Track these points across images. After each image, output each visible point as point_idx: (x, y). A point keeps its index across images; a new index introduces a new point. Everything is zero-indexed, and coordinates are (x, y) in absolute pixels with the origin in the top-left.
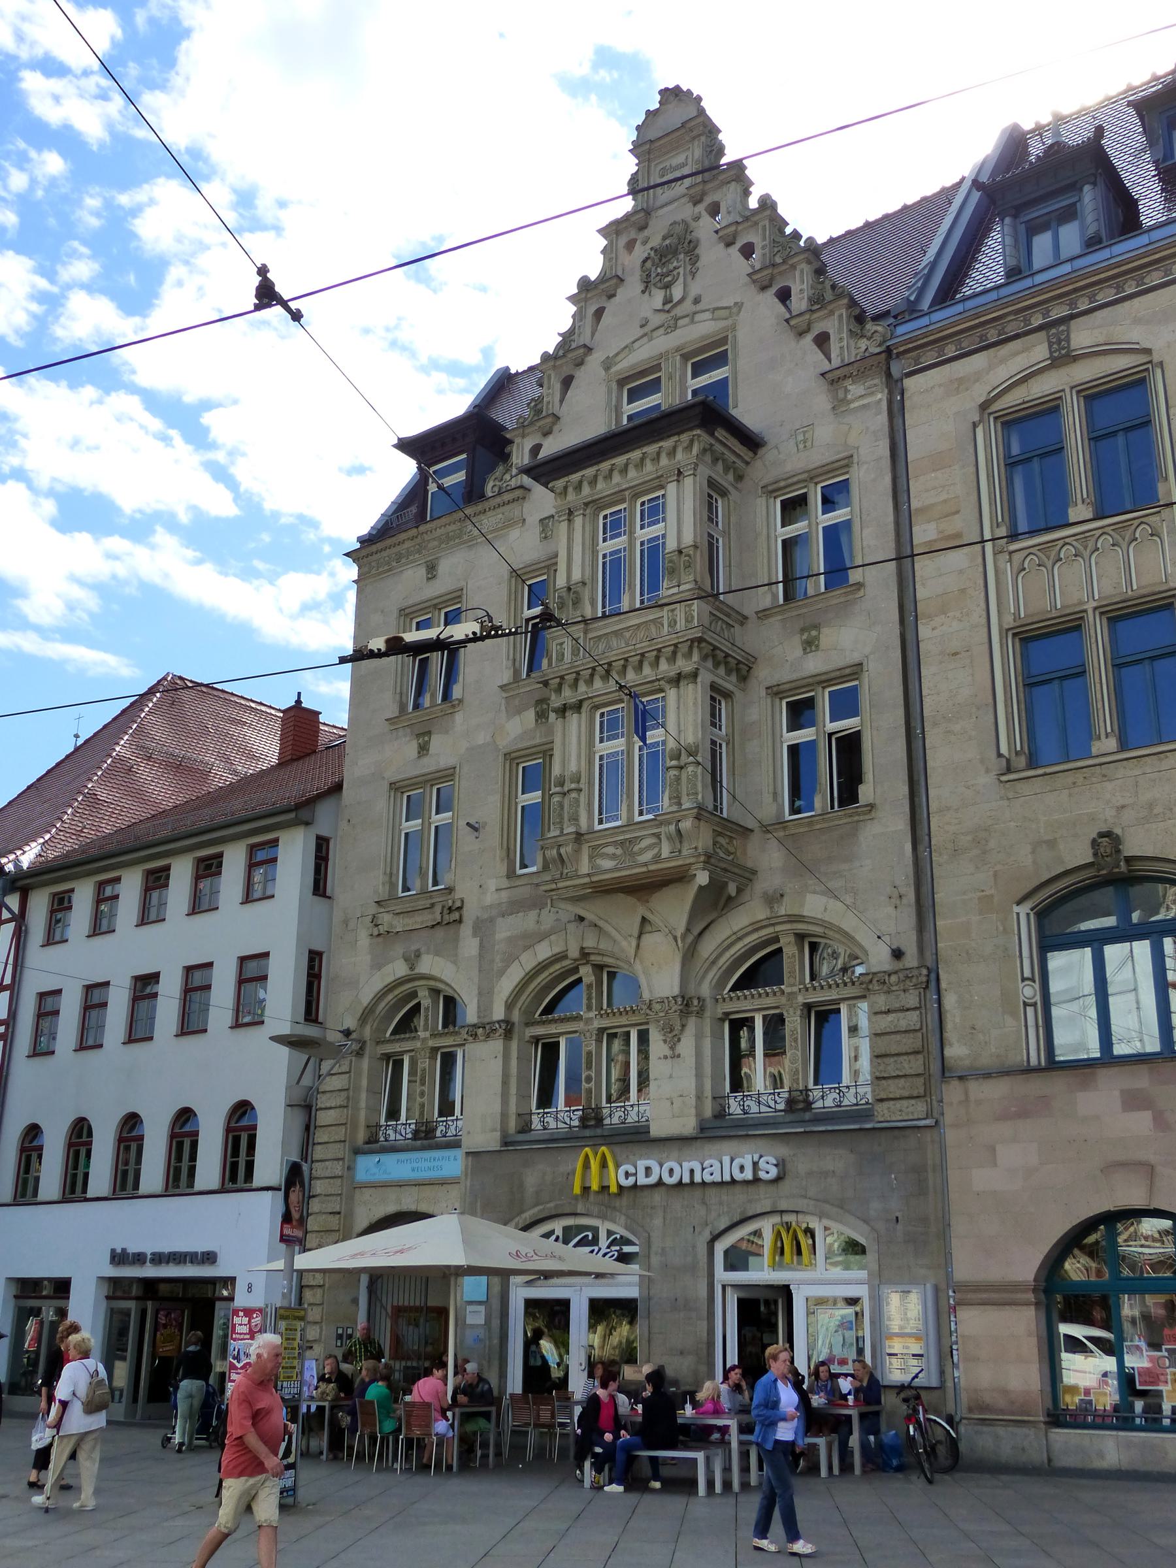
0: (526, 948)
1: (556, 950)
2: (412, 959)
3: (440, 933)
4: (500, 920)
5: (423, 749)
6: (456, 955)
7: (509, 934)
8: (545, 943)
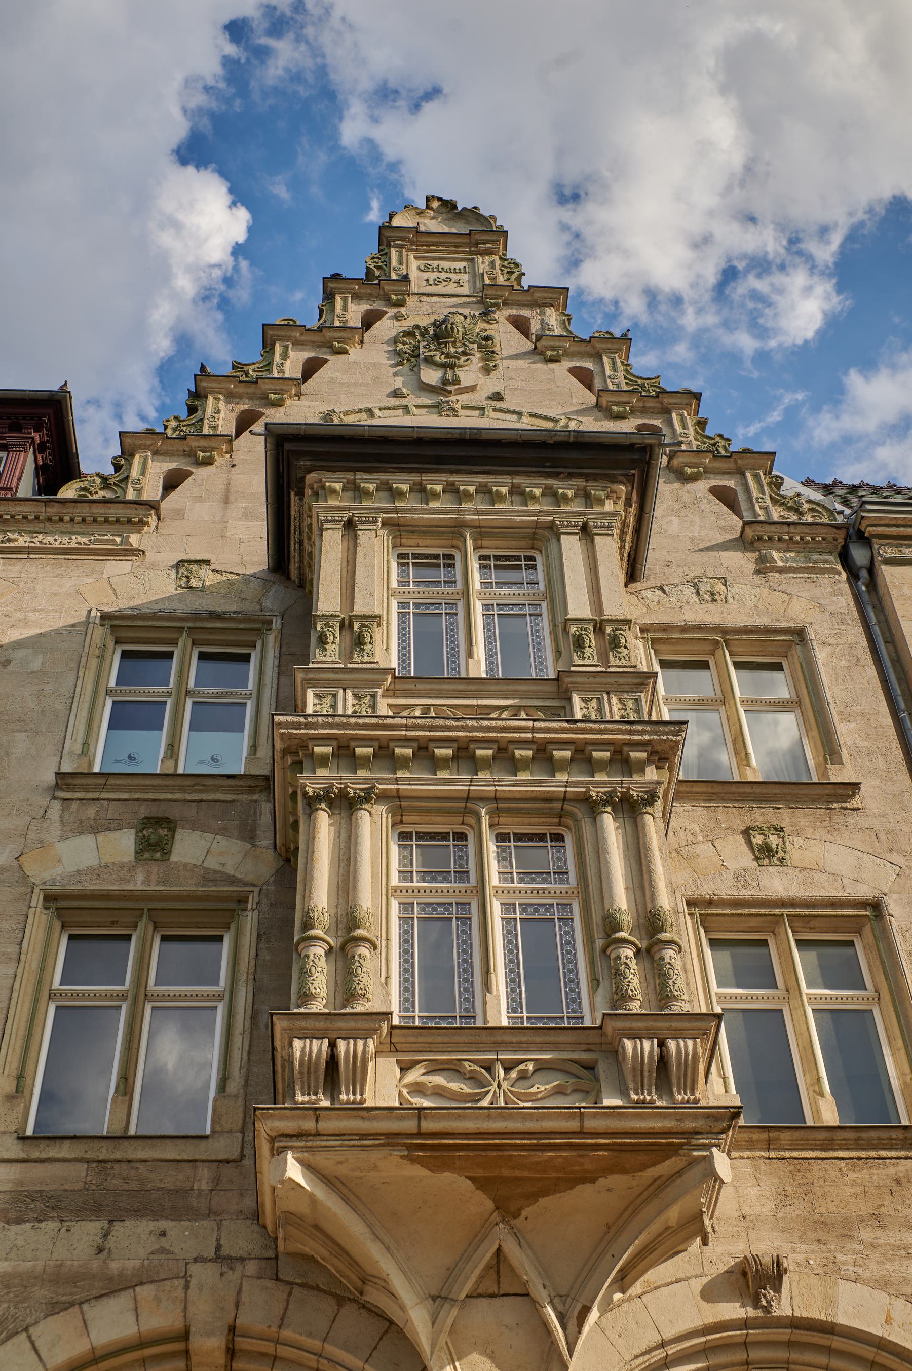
0: (55, 1308)
8: (123, 1300)
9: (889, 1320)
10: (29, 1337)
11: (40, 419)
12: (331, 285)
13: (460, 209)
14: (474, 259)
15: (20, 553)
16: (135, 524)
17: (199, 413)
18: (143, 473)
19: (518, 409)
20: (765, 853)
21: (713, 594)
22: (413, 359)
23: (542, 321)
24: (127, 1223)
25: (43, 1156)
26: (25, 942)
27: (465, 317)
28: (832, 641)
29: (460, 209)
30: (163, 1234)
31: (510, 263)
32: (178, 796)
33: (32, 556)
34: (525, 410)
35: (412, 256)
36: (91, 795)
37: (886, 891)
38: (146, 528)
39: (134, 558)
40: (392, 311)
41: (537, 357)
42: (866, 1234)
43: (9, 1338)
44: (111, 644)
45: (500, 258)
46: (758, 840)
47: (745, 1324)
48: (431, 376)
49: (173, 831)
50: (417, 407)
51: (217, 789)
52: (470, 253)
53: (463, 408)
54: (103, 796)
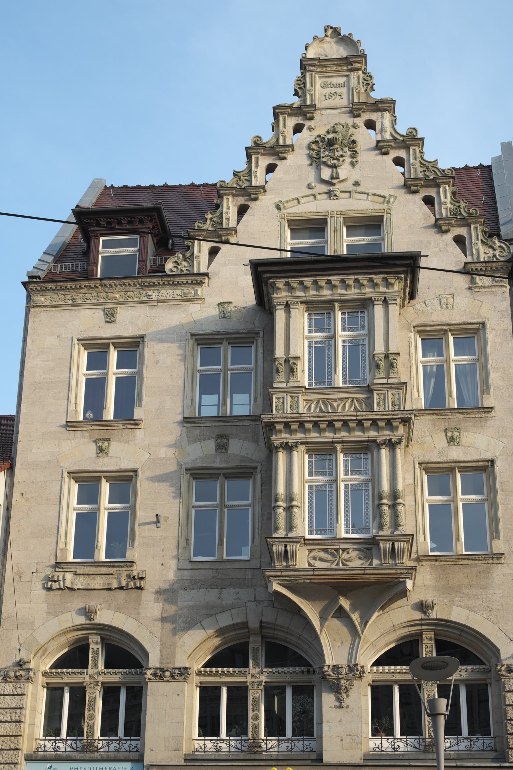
0: (208, 616)
1: (237, 621)
2: (88, 613)
3: (121, 595)
4: (181, 592)
5: (101, 451)
6: (138, 613)
7: (191, 603)
8: (228, 613)
9: (468, 619)
10: (201, 625)
11: (151, 217)
12: (277, 111)
13: (342, 35)
14: (349, 75)
15: (154, 303)
16: (199, 283)
17: (220, 208)
18: (200, 252)
19: (367, 191)
20: (451, 440)
21: (447, 304)
22: (317, 161)
23: (382, 123)
24: (226, 589)
25: (198, 568)
26: (181, 489)
27: (343, 127)
28: (496, 328)
29: (342, 35)
30: (238, 593)
31: (367, 76)
32: (229, 424)
33: (159, 304)
34: (370, 191)
35: (317, 78)
36: (197, 425)
37: (497, 455)
38: (204, 284)
39: (201, 302)
40: (307, 124)
41: (377, 152)
42: (465, 591)
43: (195, 625)
44: (196, 347)
45: (363, 72)
46: (449, 434)
47: (421, 620)
48: (326, 173)
49: (228, 440)
50: (319, 194)
51: (243, 420)
52: (348, 70)
53: (341, 192)
54: (202, 425)
